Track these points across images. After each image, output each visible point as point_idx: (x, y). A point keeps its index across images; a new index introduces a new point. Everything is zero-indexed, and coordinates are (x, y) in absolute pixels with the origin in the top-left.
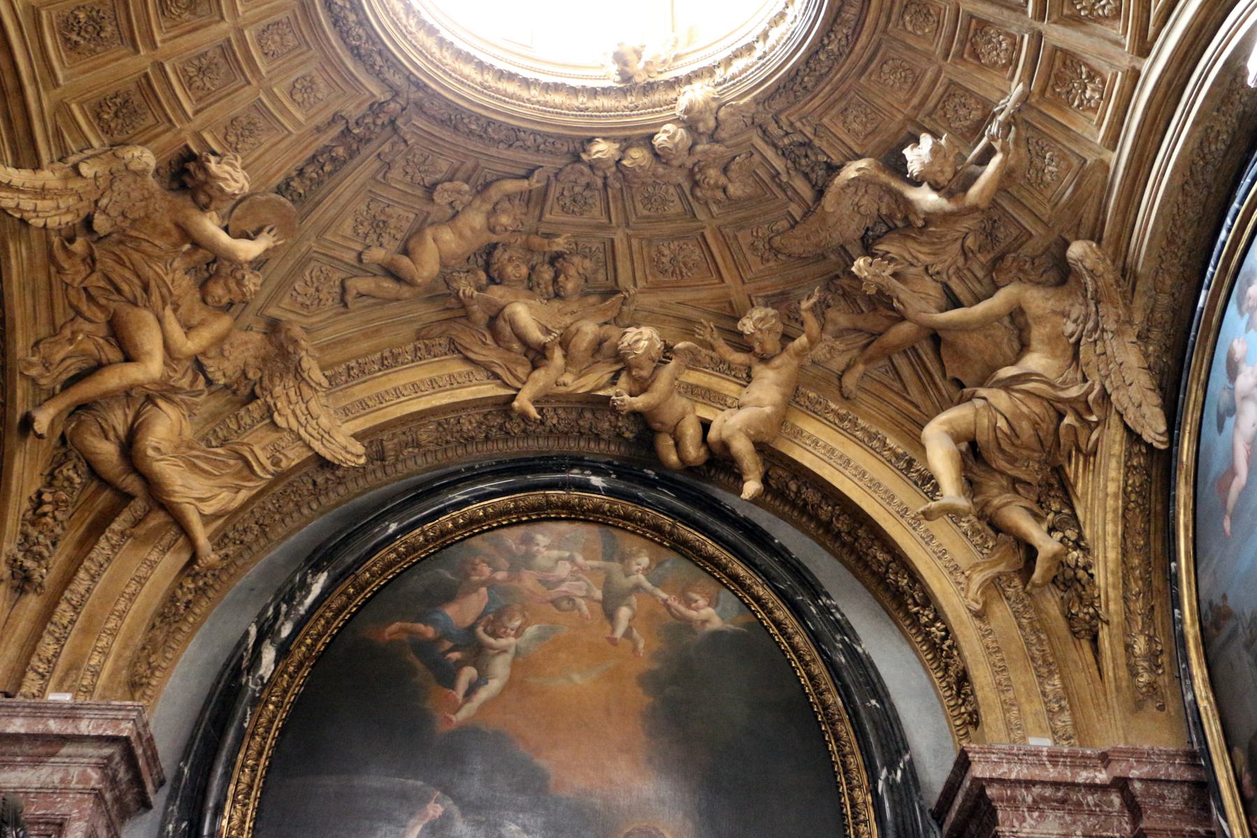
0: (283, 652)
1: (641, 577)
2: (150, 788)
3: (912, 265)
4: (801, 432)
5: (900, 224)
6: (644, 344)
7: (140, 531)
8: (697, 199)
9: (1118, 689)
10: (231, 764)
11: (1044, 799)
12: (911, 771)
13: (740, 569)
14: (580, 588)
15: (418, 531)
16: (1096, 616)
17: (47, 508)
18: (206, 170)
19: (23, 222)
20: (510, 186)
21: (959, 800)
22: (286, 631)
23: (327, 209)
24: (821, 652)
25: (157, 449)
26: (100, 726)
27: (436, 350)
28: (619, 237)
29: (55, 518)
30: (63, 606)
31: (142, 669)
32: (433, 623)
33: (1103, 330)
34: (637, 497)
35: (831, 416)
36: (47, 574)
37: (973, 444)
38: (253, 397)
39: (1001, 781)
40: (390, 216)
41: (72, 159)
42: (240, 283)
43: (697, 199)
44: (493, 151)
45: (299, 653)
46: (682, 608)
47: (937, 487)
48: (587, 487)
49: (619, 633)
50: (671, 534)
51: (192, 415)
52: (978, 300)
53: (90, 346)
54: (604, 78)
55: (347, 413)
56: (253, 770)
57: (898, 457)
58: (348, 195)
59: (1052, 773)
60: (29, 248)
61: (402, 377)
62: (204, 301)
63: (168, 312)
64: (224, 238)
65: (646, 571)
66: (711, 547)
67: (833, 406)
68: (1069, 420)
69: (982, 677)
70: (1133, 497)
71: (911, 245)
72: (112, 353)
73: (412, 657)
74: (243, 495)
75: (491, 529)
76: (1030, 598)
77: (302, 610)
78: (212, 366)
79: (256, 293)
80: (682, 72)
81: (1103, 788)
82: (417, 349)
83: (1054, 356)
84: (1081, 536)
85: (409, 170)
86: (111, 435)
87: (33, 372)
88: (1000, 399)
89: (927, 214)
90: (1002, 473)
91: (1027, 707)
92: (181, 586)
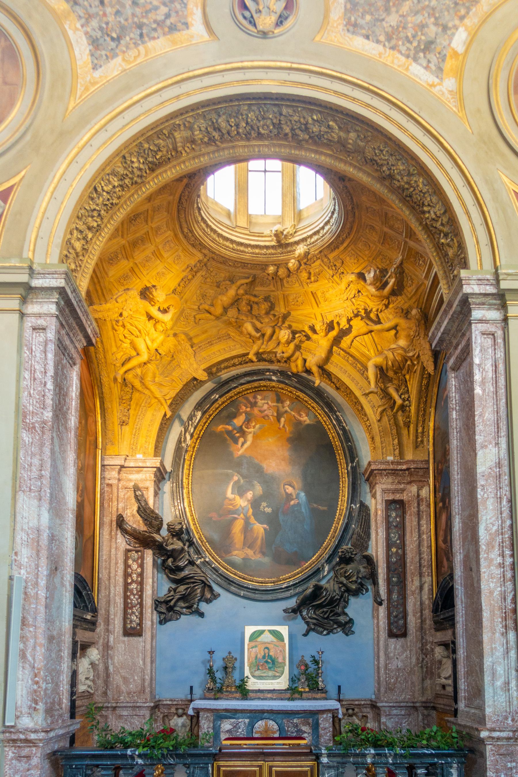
11: (389, 473)
32: (231, 425)
37: (382, 367)
48: (271, 380)
49: (281, 426)
54: (272, 241)
59: (391, 467)
65: (289, 406)
66: (307, 398)
69: (378, 439)
77: (195, 424)
80: (297, 239)
81: (404, 470)
84: (409, 397)
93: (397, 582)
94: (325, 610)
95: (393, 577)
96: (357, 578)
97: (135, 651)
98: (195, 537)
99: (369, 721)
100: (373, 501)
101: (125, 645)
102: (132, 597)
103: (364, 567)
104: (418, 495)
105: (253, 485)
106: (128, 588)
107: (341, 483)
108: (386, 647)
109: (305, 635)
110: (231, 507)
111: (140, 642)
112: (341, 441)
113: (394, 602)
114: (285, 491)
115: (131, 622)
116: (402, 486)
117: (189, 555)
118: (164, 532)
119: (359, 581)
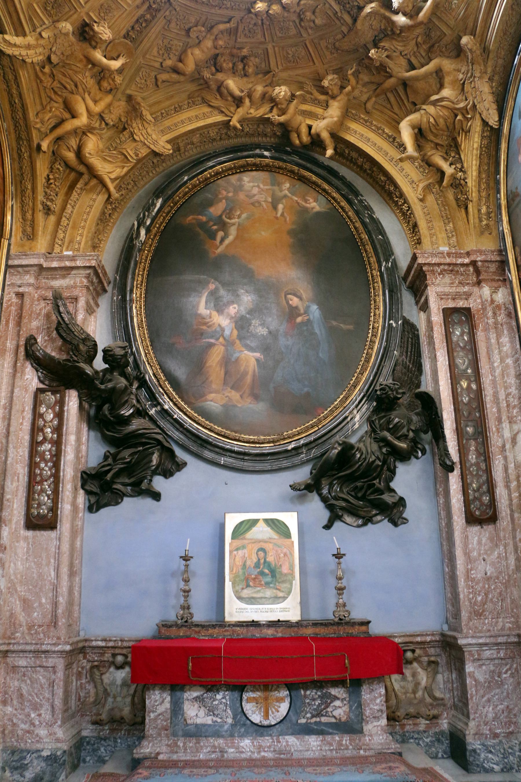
0: (148, 230)
1: (287, 192)
2: (106, 284)
3: (395, 51)
4: (350, 128)
5: (389, 33)
6: (283, 93)
7: (88, 187)
8: (302, 27)
9: (475, 227)
10: (134, 274)
11: (445, 270)
12: (395, 262)
13: (326, 187)
14: (262, 198)
15: (196, 179)
16: (467, 199)
17: (52, 181)
18: (93, 30)
19: (24, 61)
20: (222, 27)
21: (412, 272)
22: (148, 222)
23: (146, 44)
24: (359, 218)
25: (90, 154)
26: (83, 263)
27: (197, 103)
28: (270, 47)
29: (55, 185)
30: (64, 219)
31: (96, 241)
32: (205, 215)
33: (475, 77)
34: (283, 159)
35: (361, 121)
36: (56, 206)
37: (420, 130)
38: (125, 129)
39: (429, 264)
40: (172, 45)
41: (38, 30)
42: (113, 80)
43: (302, 27)
44: (213, 11)
45: (154, 230)
46: (304, 203)
47: (405, 148)
49: (279, 215)
50: (298, 173)
51: (101, 138)
52: (423, 66)
53: (58, 113)
55: (163, 132)
56: (142, 275)
57: (390, 137)
58: (154, 36)
59: (448, 260)
60: (28, 73)
61: (185, 115)
62: (100, 89)
63: (86, 95)
64: (104, 60)
65: (288, 189)
66: (314, 178)
67: (362, 116)
68: (459, 117)
69: (422, 225)
70: (484, 149)
71: (394, 42)
72: (67, 115)
73: (198, 229)
74: (125, 170)
75: (225, 176)
76: (442, 193)
77: (154, 214)
78: (107, 117)
79: (121, 84)
81: (467, 265)
82: (189, 103)
83: (454, 90)
84: (463, 167)
85: (178, 23)
86: (71, 150)
87: (38, 126)
88: (431, 109)
89: (401, 27)
90: (432, 141)
91: (440, 236)
92: (106, 208)
93: (474, 434)
94: (359, 484)
95: (467, 426)
96: (408, 431)
97: (44, 555)
98: (147, 372)
99: (440, 669)
100: (422, 315)
101: (28, 544)
102: (42, 465)
103: (417, 414)
104: (492, 301)
105: (238, 296)
106: (36, 451)
107: (372, 290)
108: (466, 539)
109: (328, 527)
110: (204, 327)
111: (52, 539)
112: (369, 233)
113: (472, 465)
114: (288, 302)
115: (39, 505)
116: (466, 289)
117: (138, 401)
118: (99, 364)
119: (411, 434)
